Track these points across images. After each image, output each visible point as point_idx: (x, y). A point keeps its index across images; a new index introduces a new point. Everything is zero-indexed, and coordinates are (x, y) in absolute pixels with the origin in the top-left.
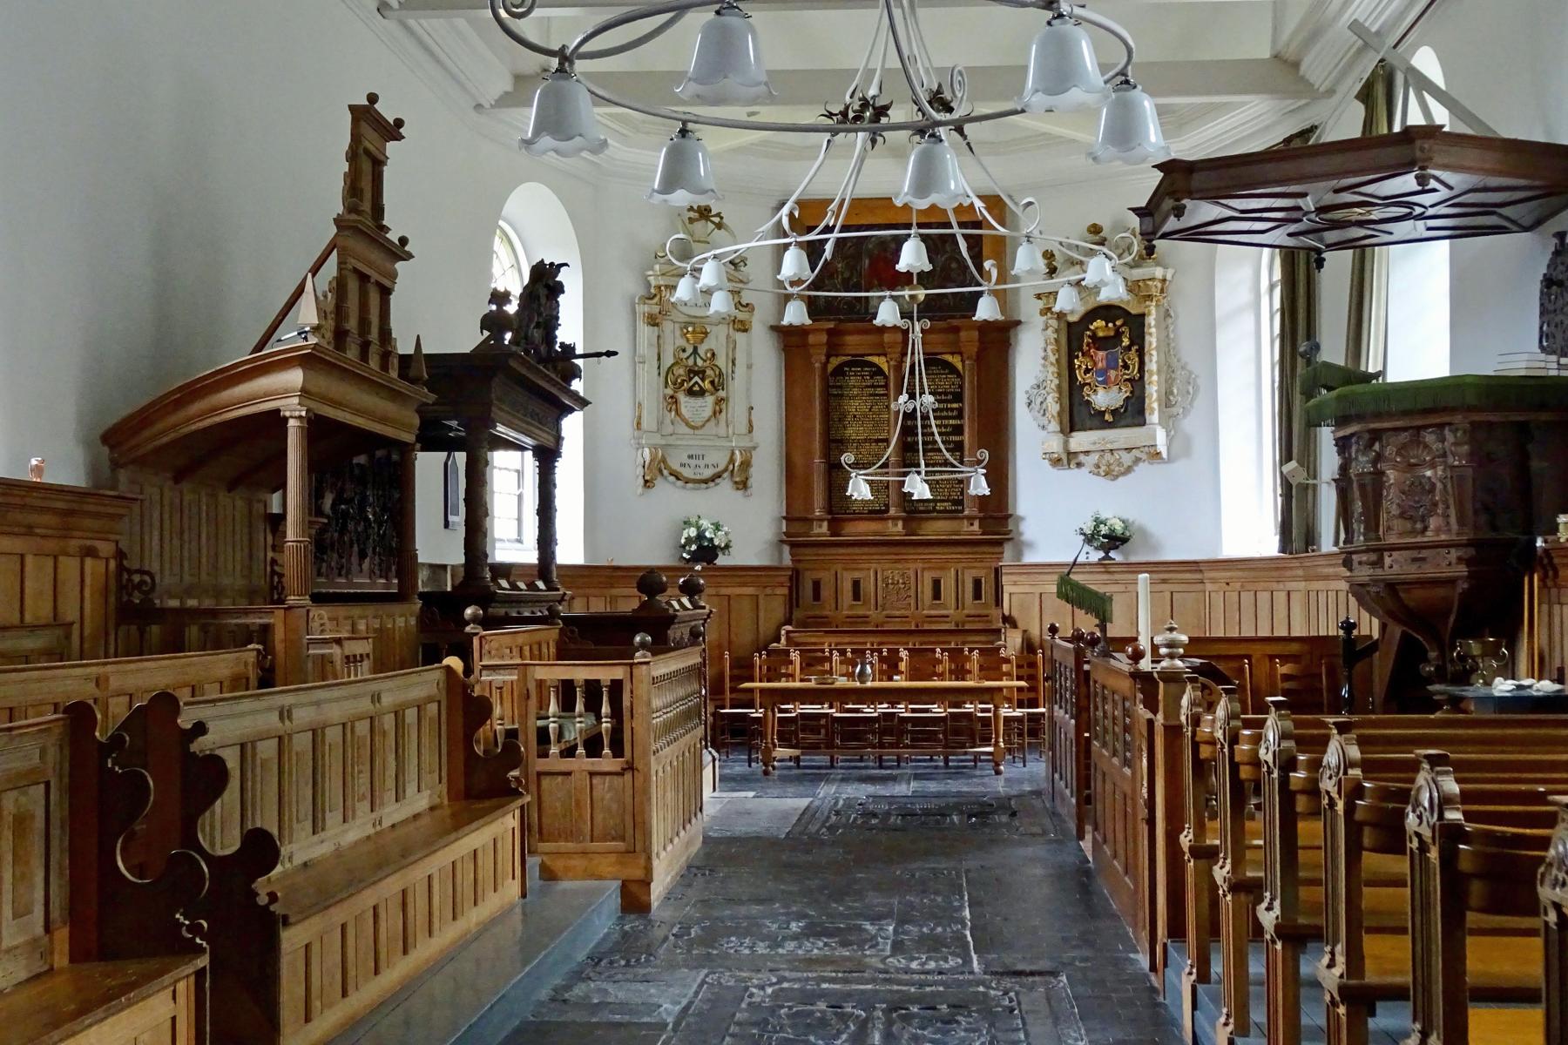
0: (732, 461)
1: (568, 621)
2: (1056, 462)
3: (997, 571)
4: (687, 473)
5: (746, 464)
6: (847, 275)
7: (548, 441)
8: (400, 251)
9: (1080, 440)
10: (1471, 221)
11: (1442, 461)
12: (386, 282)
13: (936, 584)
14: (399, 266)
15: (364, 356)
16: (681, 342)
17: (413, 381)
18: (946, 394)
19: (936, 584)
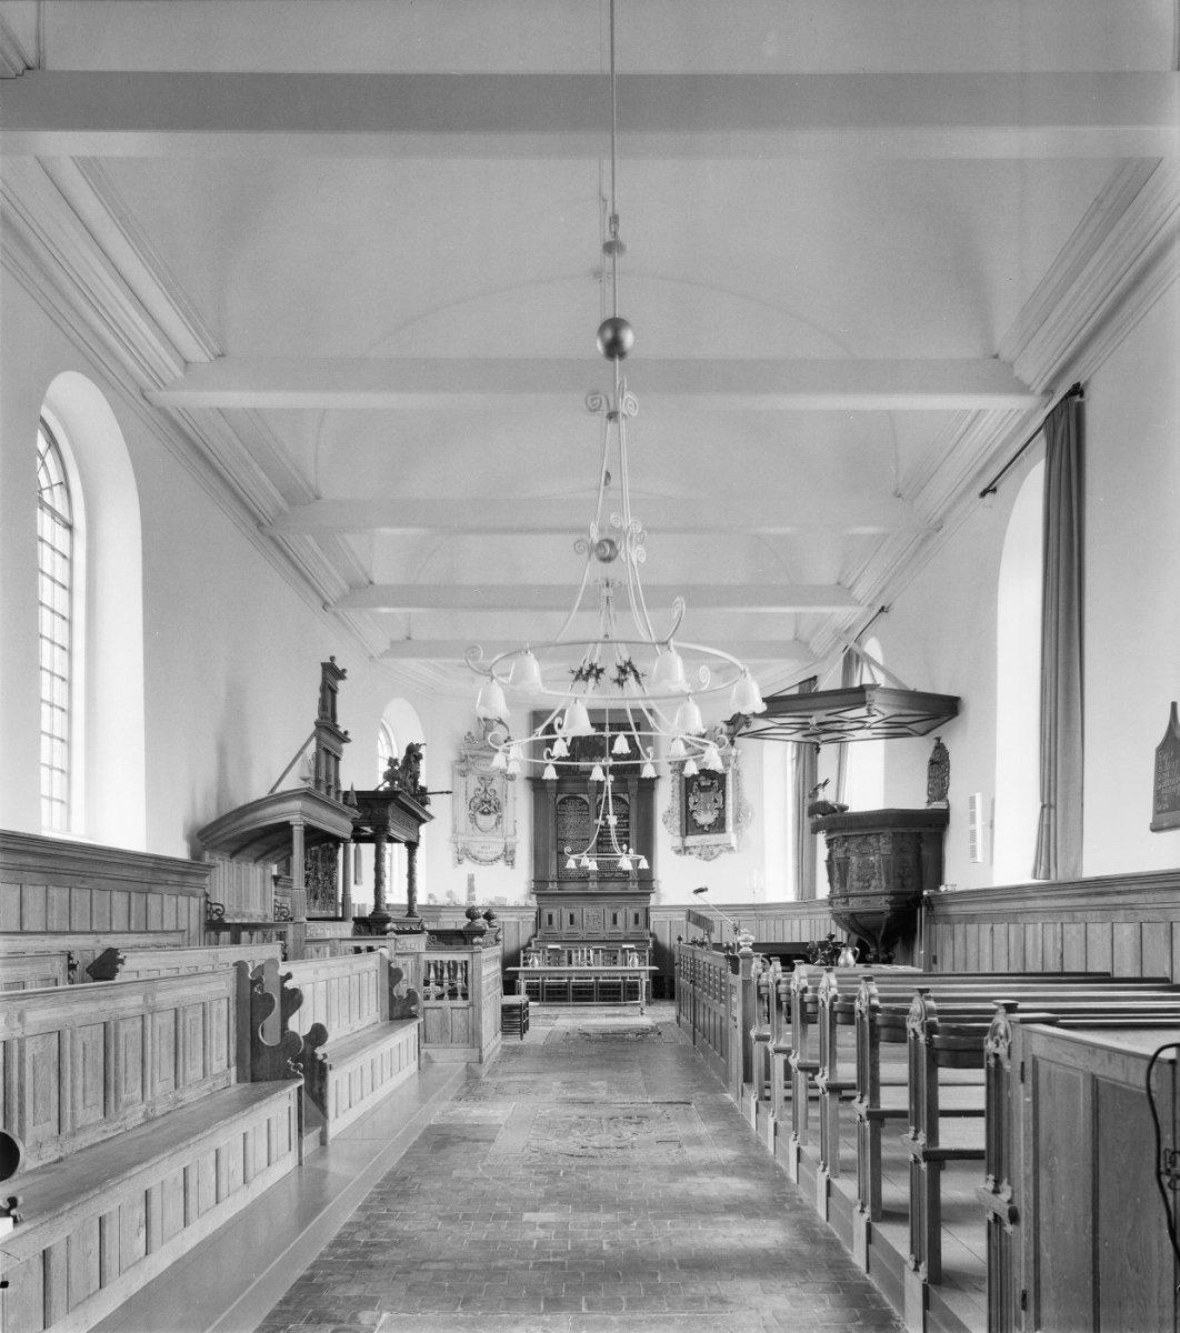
0: (505, 850)
1: (431, 932)
2: (678, 852)
3: (647, 910)
4: (481, 856)
5: (513, 852)
7: (414, 839)
8: (343, 738)
9: (691, 840)
10: (895, 730)
11: (879, 852)
12: (338, 754)
14: (344, 746)
15: (328, 793)
16: (479, 786)
17: (350, 806)
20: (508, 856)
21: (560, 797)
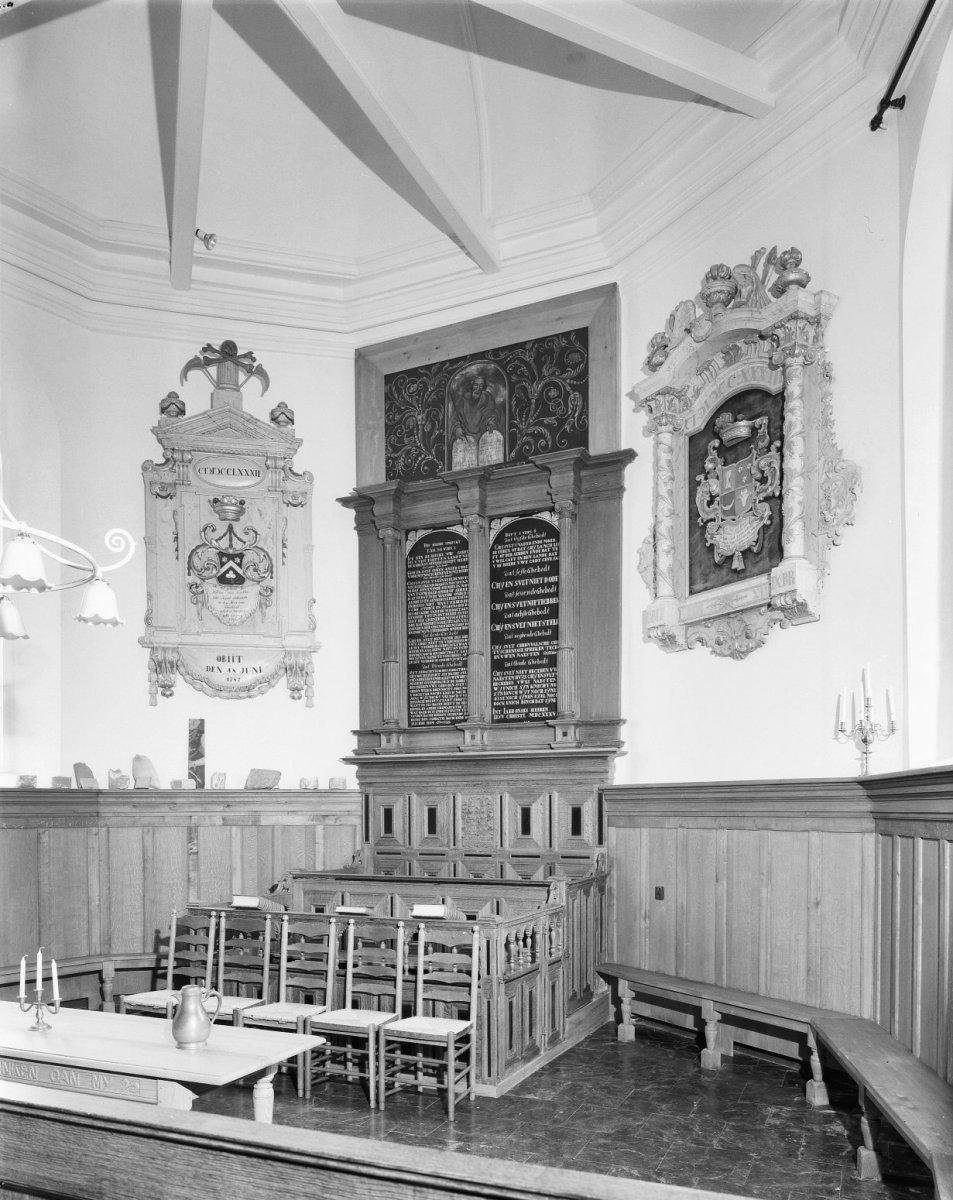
6: (428, 429)
18: (542, 564)
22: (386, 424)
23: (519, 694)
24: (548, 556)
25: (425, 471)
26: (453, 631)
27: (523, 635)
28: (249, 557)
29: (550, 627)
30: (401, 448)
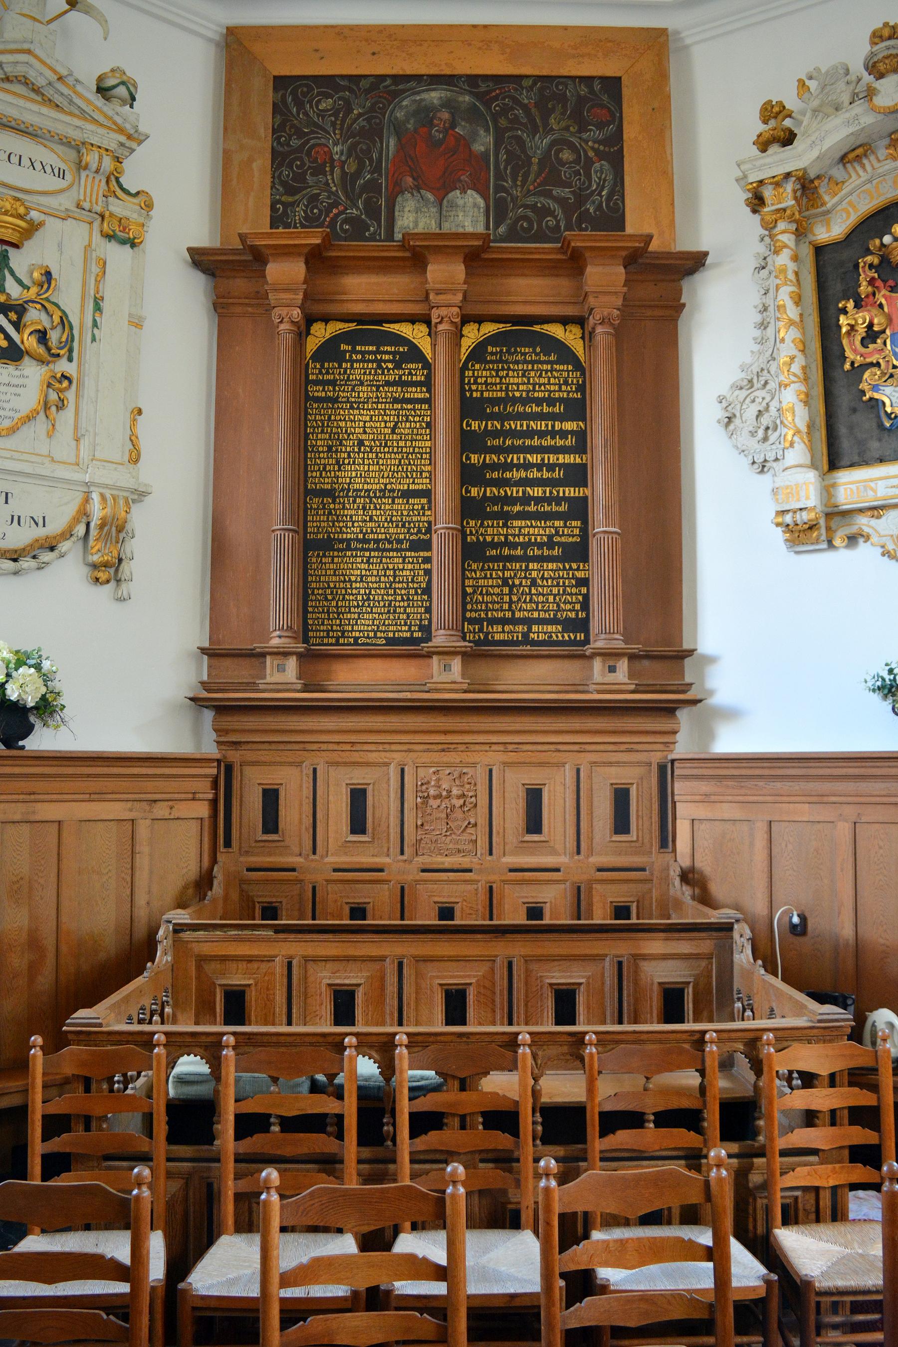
0: (83, 513)
3: (665, 773)
5: (116, 529)
6: (351, 167)
9: (855, 484)
13: (534, 797)
18: (551, 402)
19: (534, 797)
20: (105, 548)
21: (321, 333)
22: (273, 148)
23: (511, 602)
24: (560, 390)
25: (346, 231)
26: (393, 491)
27: (517, 508)
28: (35, 316)
29: (564, 498)
30: (299, 190)
